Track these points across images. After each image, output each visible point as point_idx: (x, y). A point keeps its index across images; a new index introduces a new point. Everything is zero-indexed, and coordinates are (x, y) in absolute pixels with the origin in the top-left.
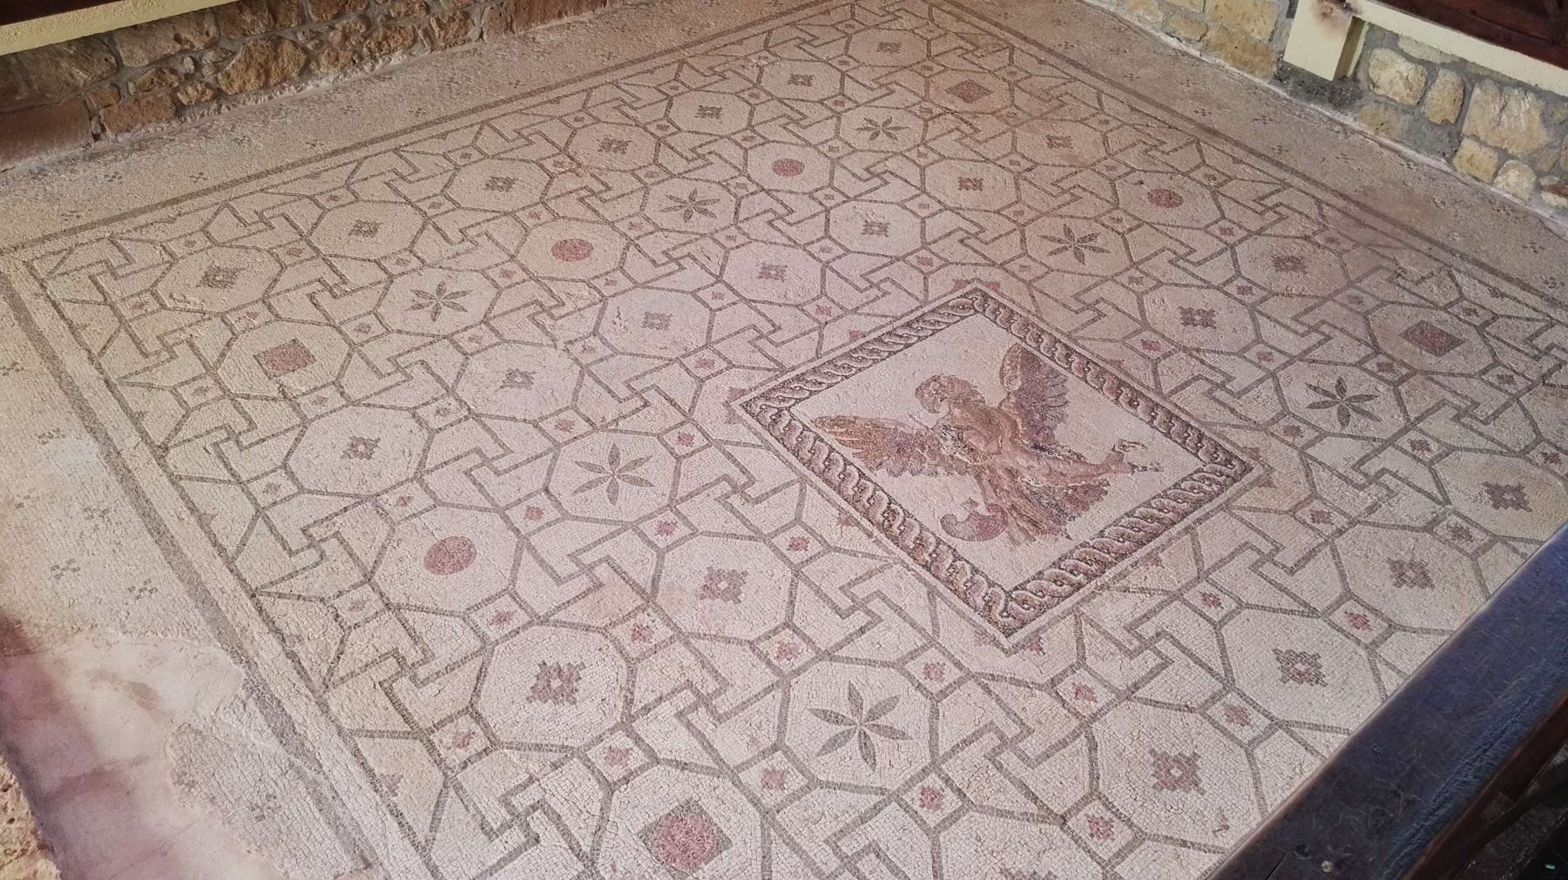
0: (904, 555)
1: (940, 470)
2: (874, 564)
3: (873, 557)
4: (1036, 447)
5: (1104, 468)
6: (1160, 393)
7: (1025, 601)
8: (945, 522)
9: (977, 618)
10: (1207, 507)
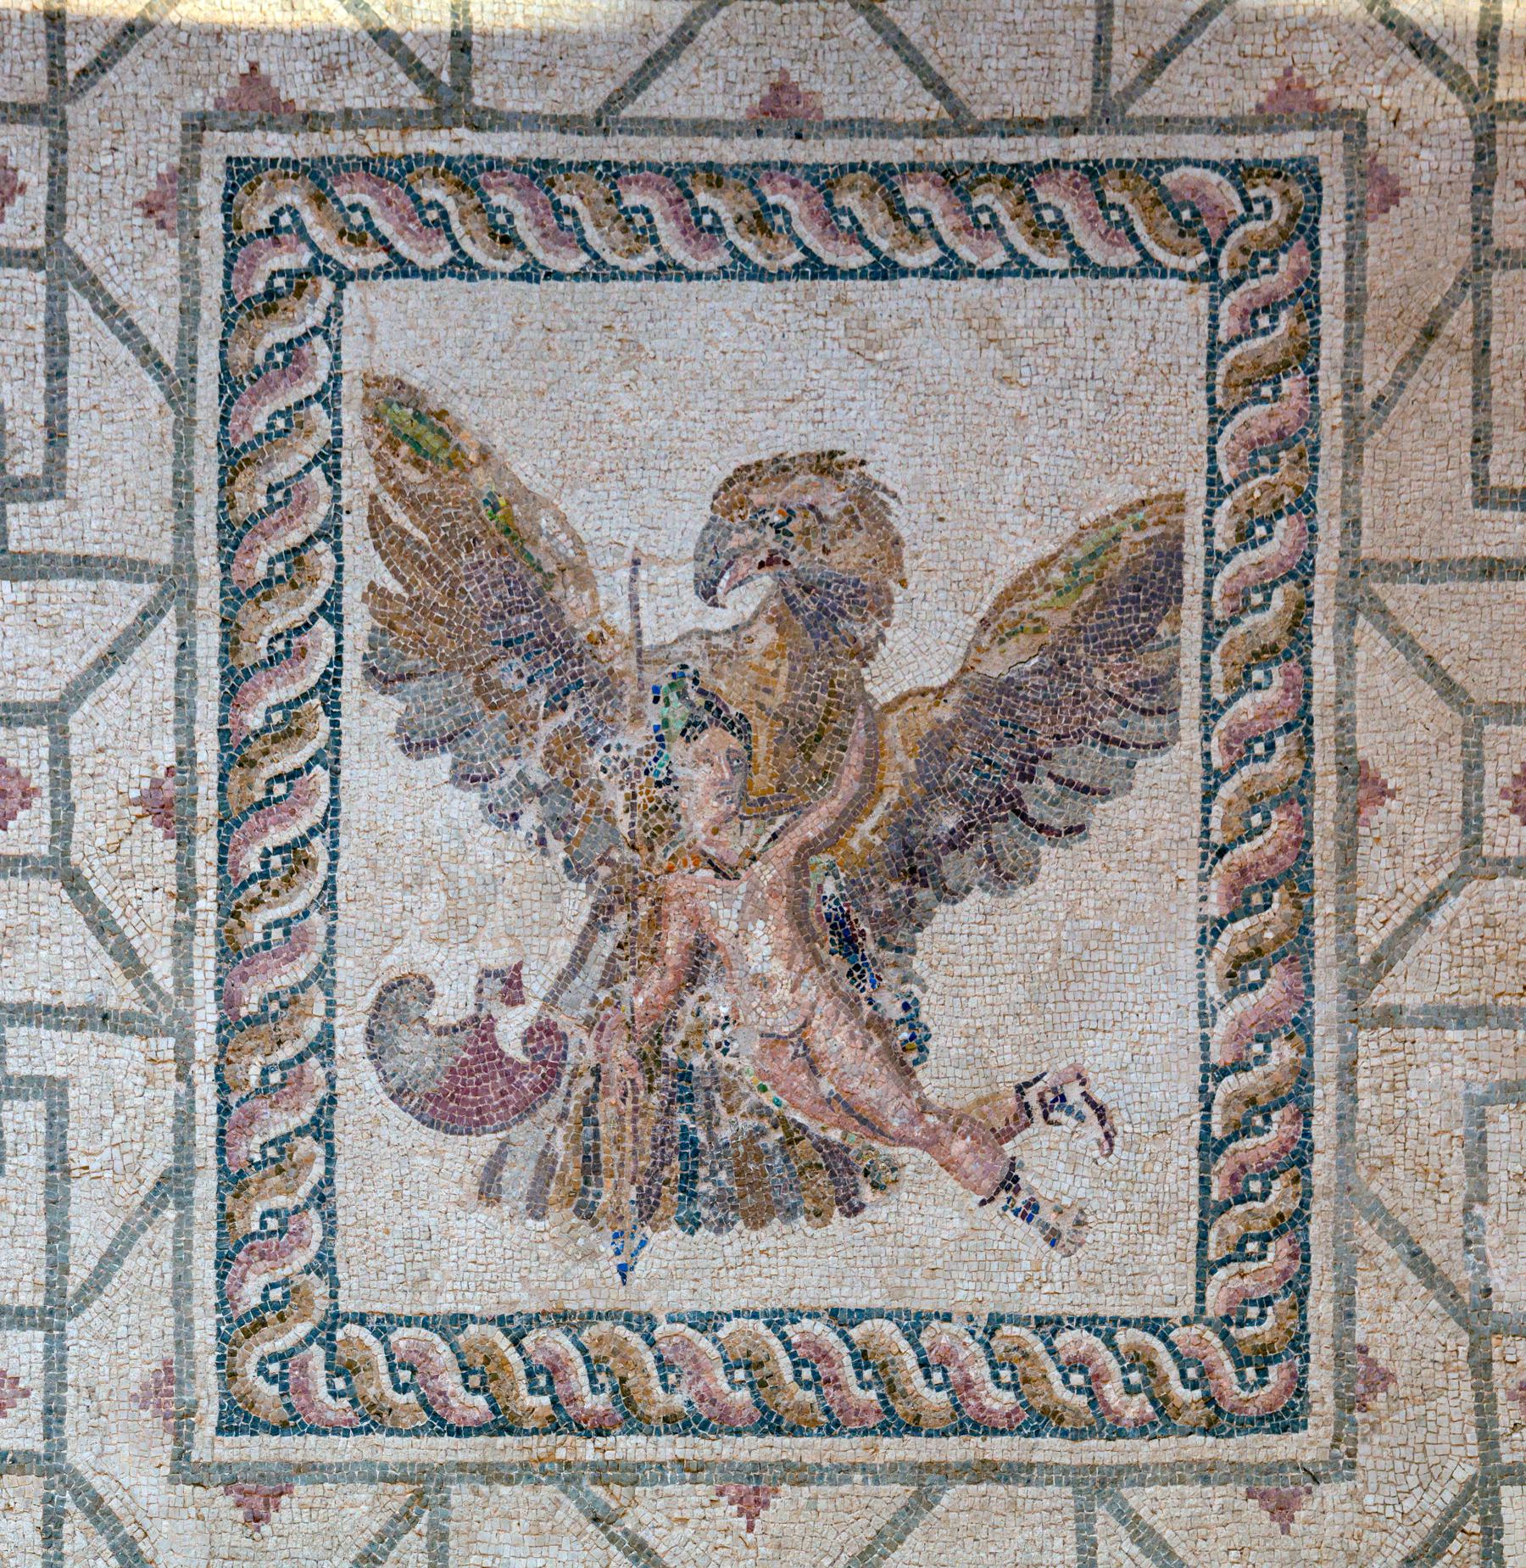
1: (531, 817)
5: (939, 1129)
7: (347, 1370)
8: (399, 998)
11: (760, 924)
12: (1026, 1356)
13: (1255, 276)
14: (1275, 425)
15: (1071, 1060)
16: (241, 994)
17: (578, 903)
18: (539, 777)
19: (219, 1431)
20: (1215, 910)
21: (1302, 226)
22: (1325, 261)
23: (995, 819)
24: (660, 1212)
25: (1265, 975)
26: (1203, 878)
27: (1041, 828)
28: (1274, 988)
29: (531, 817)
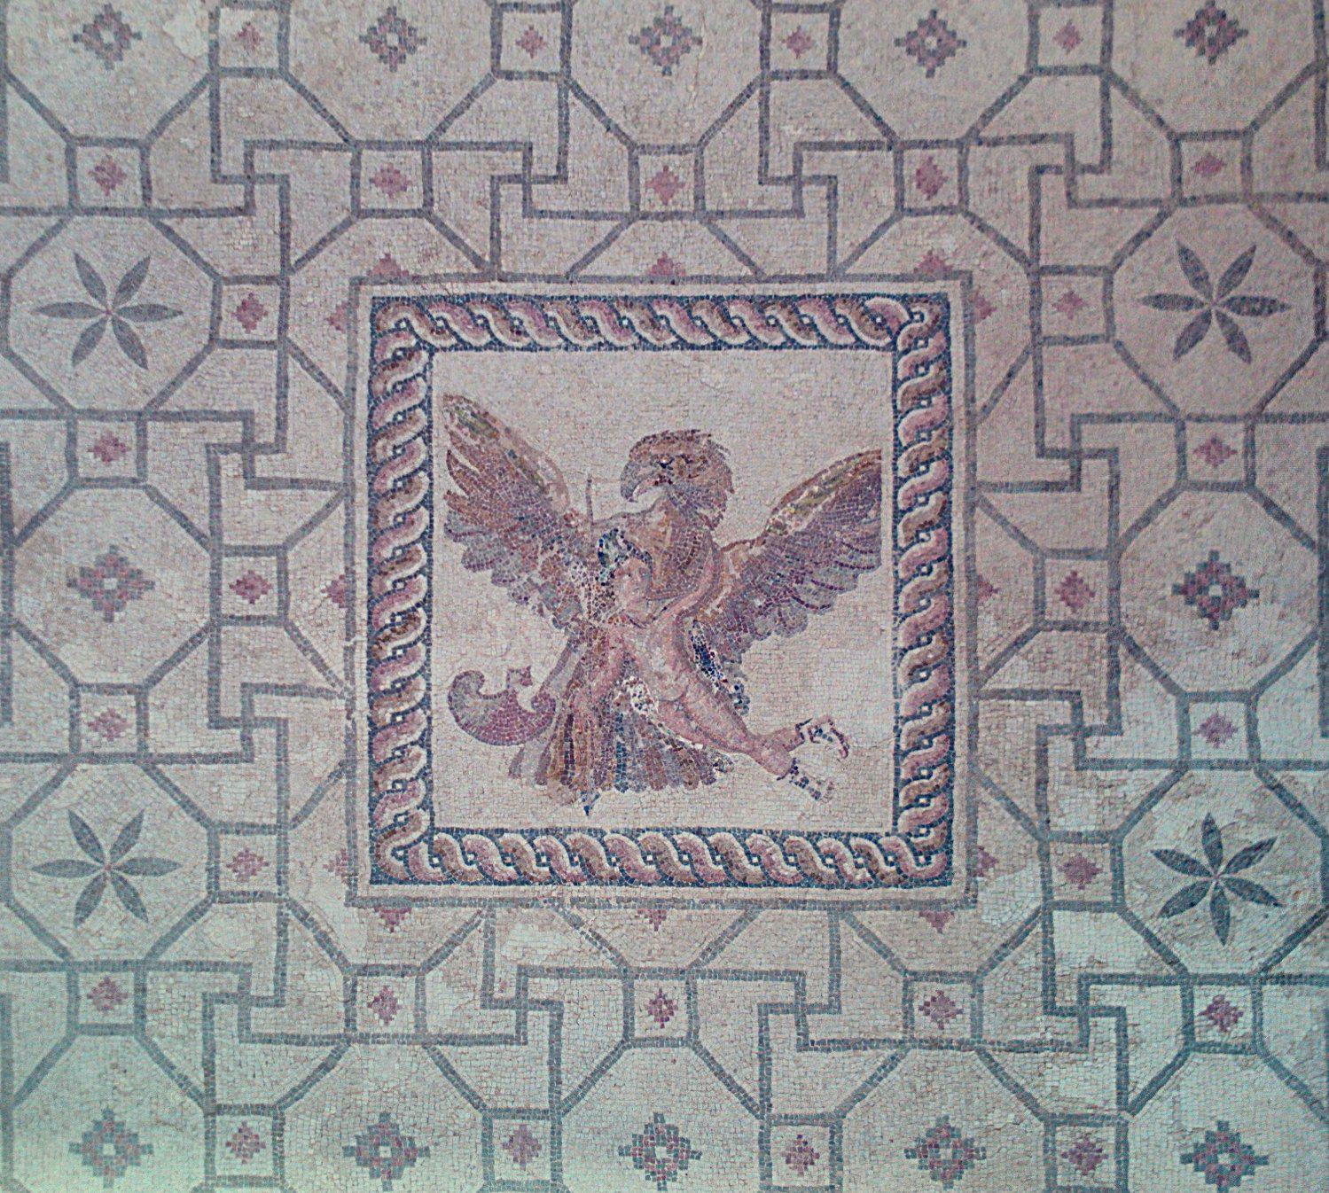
0: (362, 688)
1: (535, 598)
2: (318, 680)
3: (321, 666)
4: (700, 649)
6: (976, 681)
9: (363, 834)
10: (815, 893)
17: (560, 639)
18: (540, 582)
20: (901, 644)
25: (929, 675)
26: (895, 629)
28: (934, 680)
29: (535, 598)
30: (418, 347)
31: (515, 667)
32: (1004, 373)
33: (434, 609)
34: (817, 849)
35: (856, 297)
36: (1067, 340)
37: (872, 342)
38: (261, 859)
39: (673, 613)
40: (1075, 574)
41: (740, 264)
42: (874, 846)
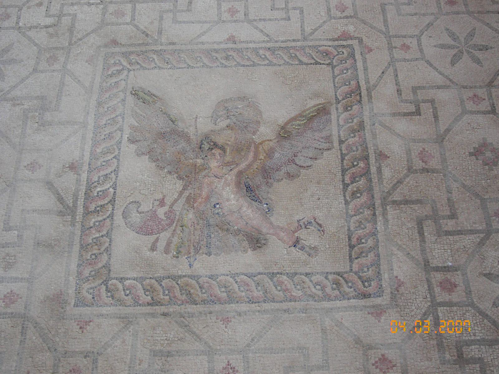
11: (228, 188)
12: (304, 282)
13: (341, 64)
14: (350, 89)
15: (312, 214)
16: (89, 206)
19: (74, 306)
21: (352, 55)
22: (358, 62)
23: (288, 165)
24: (201, 251)
27: (300, 166)
30: (123, 69)
31: (157, 198)
32: (381, 72)
33: (119, 174)
34: (311, 281)
35: (314, 47)
36: (405, 60)
37: (322, 62)
38: (18, 295)
39: (235, 171)
40: (424, 149)
41: (264, 37)
42: (341, 279)
